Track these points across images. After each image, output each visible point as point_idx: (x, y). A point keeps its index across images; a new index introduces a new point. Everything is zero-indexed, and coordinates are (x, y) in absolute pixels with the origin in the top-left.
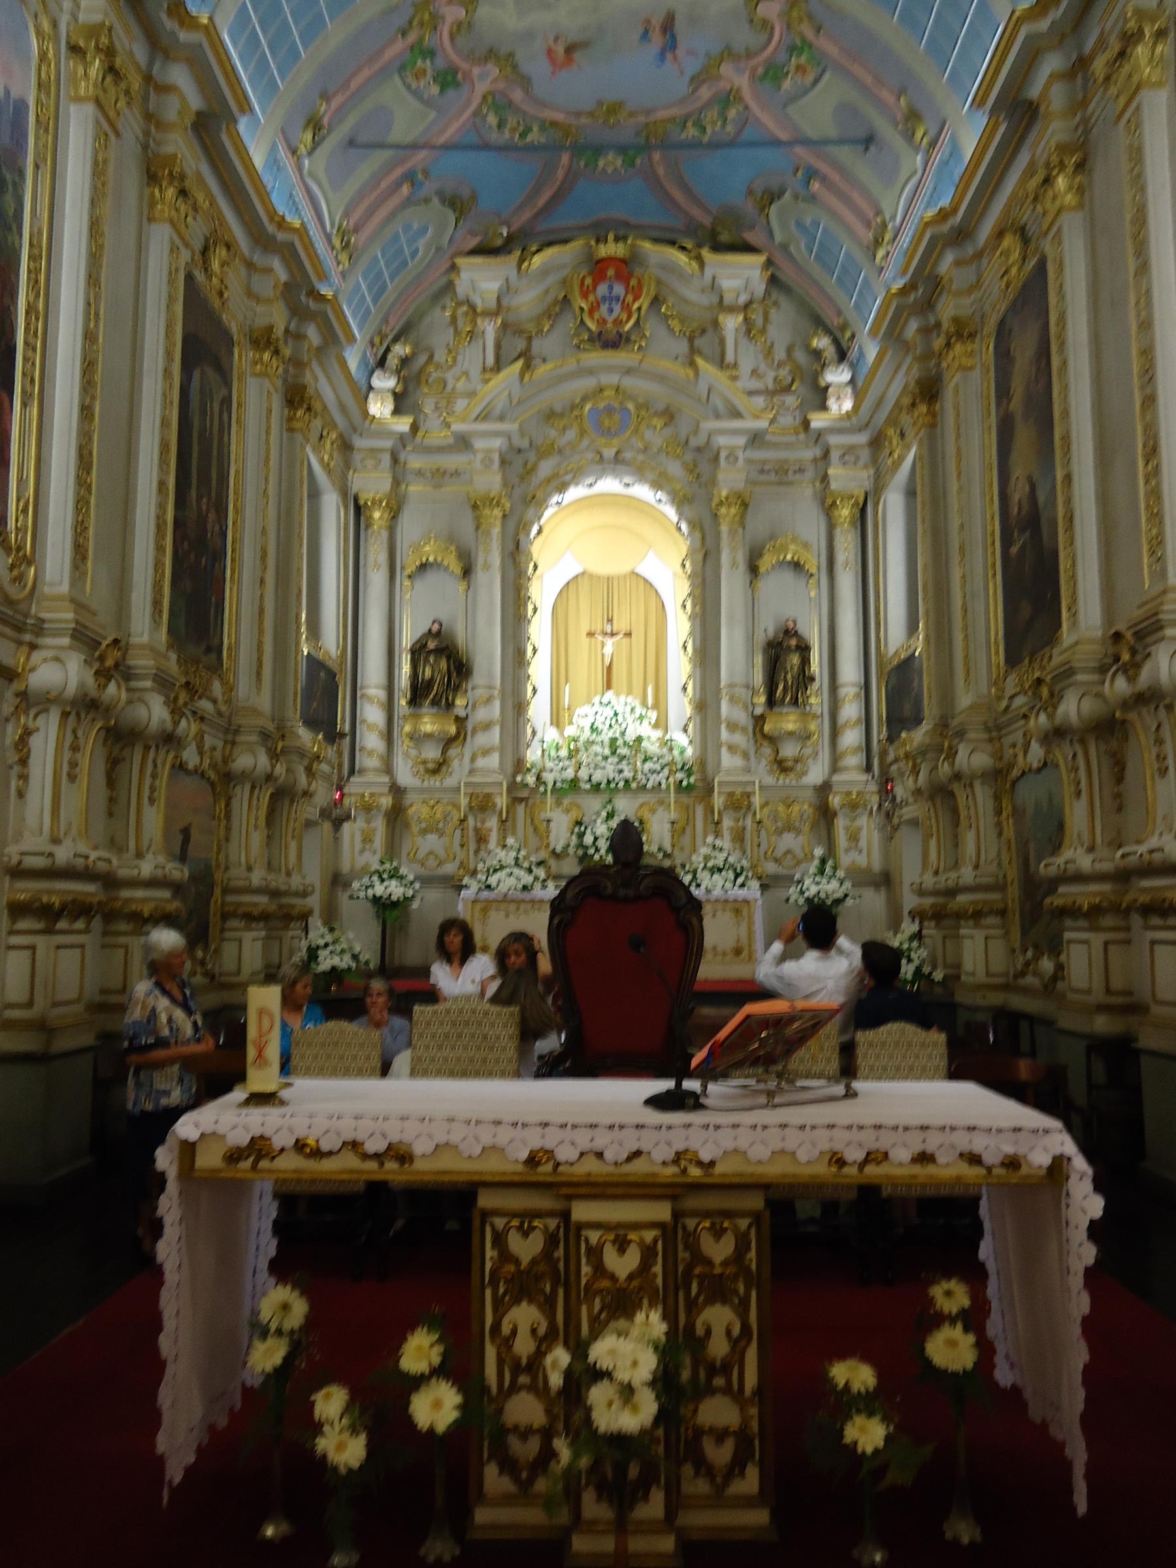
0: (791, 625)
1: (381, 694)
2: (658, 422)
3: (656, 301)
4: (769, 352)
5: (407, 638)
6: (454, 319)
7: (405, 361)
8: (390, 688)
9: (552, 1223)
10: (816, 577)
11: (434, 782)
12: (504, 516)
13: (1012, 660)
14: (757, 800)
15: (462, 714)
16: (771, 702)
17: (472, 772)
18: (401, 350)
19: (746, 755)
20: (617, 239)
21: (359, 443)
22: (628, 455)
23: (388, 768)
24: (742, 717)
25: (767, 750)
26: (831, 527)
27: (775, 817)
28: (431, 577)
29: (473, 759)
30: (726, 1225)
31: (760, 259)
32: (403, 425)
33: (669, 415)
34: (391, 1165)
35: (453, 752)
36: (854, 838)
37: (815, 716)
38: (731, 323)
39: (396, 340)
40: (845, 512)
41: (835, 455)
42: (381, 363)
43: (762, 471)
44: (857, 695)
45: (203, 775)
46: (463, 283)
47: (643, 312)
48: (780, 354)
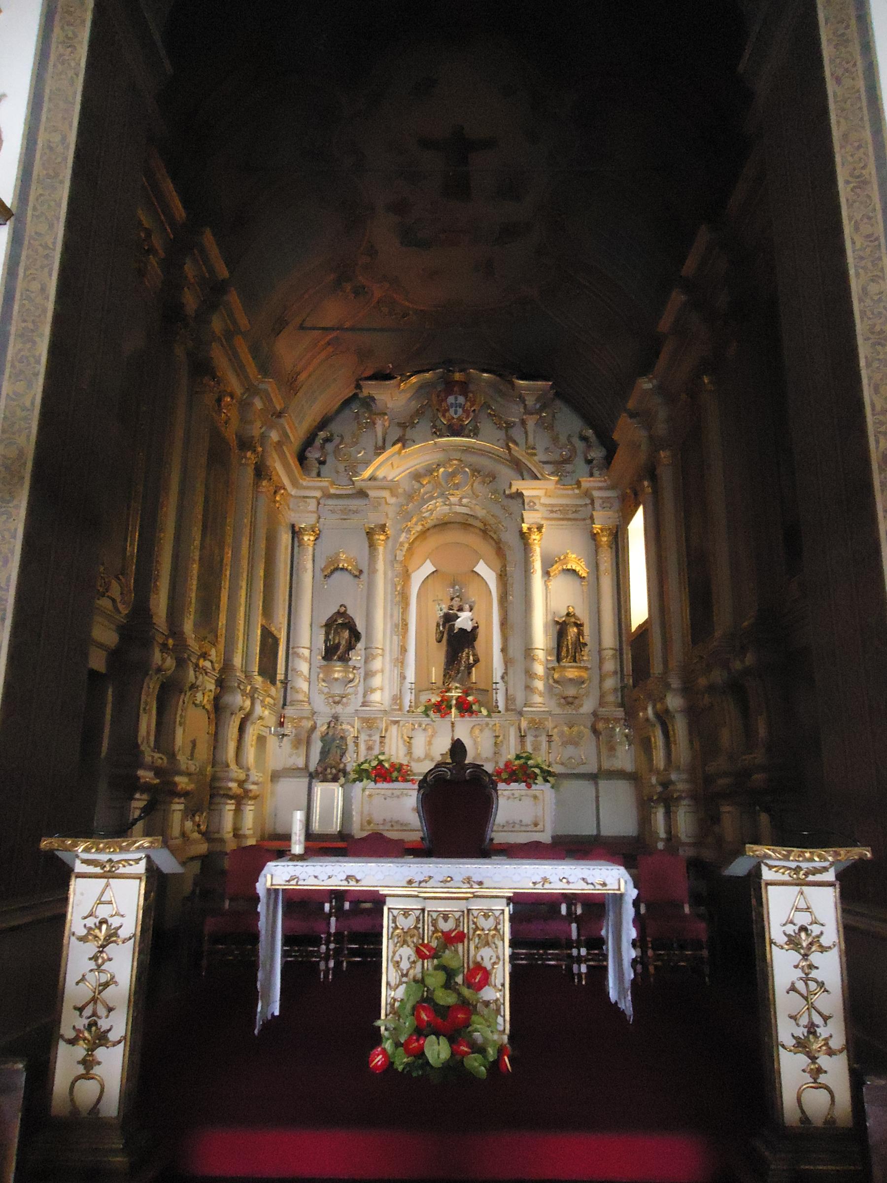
0: (571, 610)
2: (487, 479)
4: (555, 439)
9: (418, 912)
10: (587, 579)
11: (339, 709)
12: (388, 538)
13: (694, 642)
15: (358, 665)
16: (559, 660)
17: (364, 704)
20: (460, 371)
22: (465, 501)
26: (597, 547)
27: (562, 734)
29: (364, 697)
30: (490, 914)
34: (353, 883)
36: (612, 749)
37: (586, 668)
41: (597, 503)
43: (552, 512)
44: (614, 656)
45: (204, 707)
47: (477, 412)
48: (563, 439)
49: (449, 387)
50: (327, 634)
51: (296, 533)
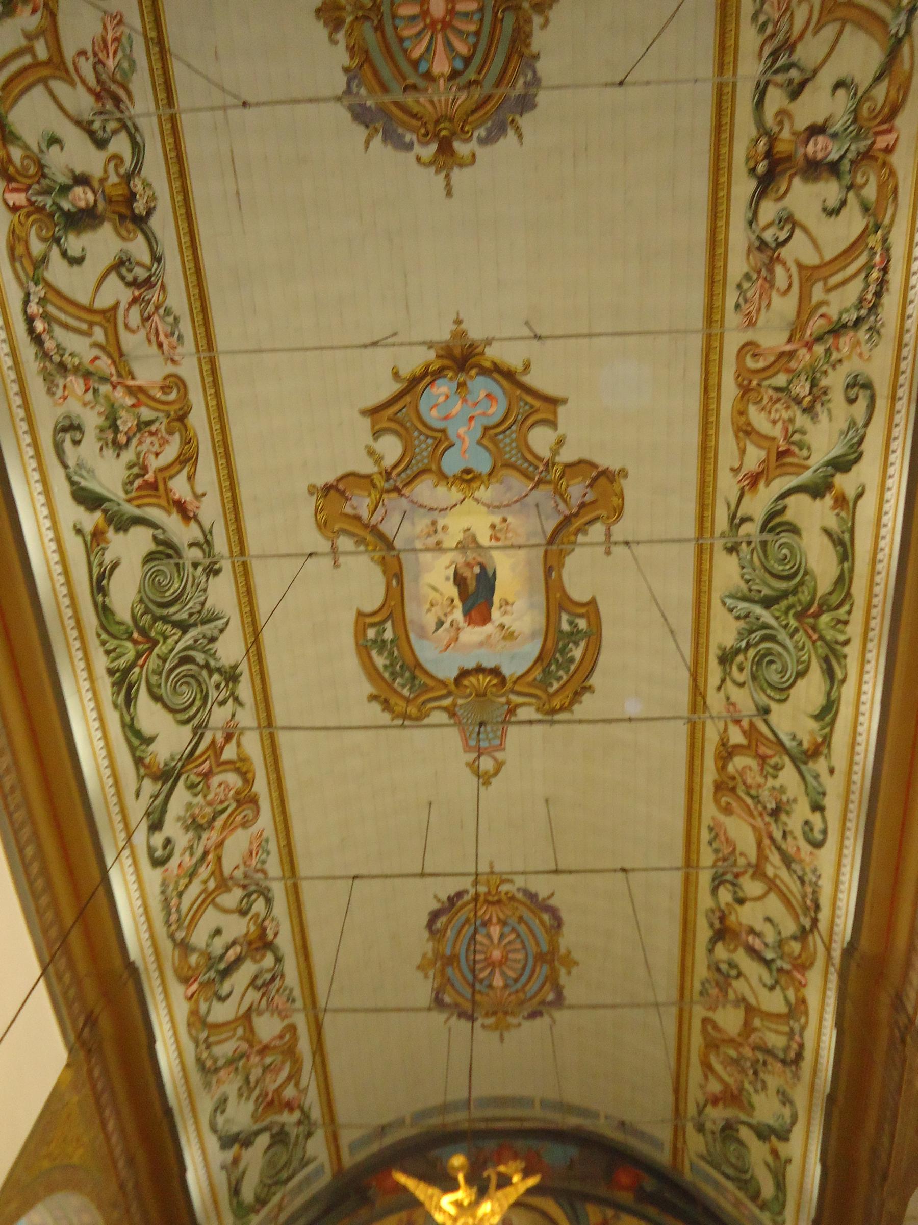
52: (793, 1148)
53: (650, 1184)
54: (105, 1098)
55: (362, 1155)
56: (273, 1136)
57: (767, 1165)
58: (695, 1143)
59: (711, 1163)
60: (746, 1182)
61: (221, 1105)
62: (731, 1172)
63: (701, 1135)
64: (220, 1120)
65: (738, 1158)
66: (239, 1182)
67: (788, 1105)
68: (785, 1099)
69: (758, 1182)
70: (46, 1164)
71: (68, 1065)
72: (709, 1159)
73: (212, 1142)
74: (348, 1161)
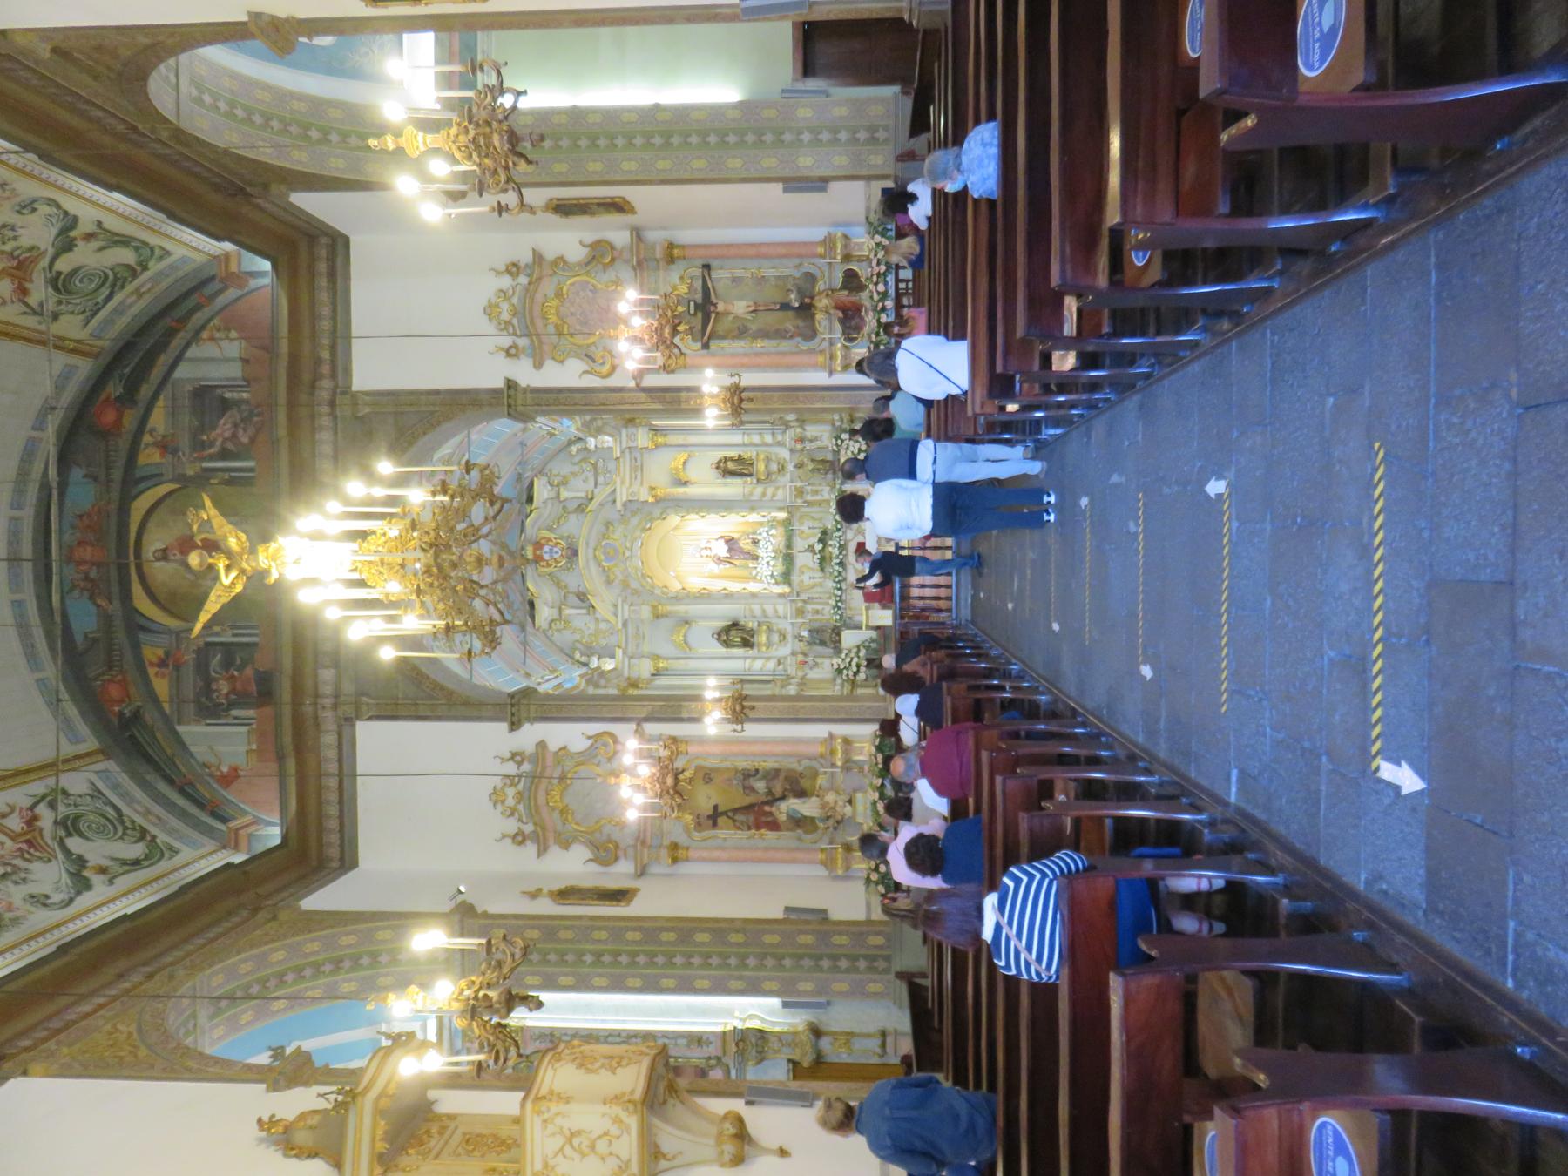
1: (748, 661)
3: (550, 529)
4: (574, 474)
5: (723, 651)
6: (558, 630)
7: (582, 655)
8: (745, 658)
11: (789, 637)
14: (799, 484)
16: (750, 475)
17: (786, 618)
18: (577, 656)
19: (777, 488)
21: (626, 674)
22: (628, 545)
23: (786, 658)
24: (759, 490)
25: (773, 477)
26: (666, 445)
28: (691, 640)
31: (536, 480)
32: (619, 653)
33: (608, 524)
35: (775, 628)
38: (564, 494)
39: (572, 658)
40: (660, 440)
41: (631, 444)
42: (586, 665)
46: (545, 626)
48: (576, 469)
49: (538, 559)
50: (734, 646)
51: (657, 673)
52: (87, 216)
53: (114, 389)
54: (56, 1024)
55: (83, 728)
56: (69, 835)
57: (101, 249)
58: (70, 326)
59: (93, 316)
60: (116, 279)
61: (41, 901)
62: (105, 292)
63: (61, 317)
64: (56, 898)
65: (91, 281)
66: (124, 863)
67: (35, 206)
68: (28, 207)
69: (119, 265)
70: (143, 1052)
71: (25, 1073)
72: (88, 314)
73: (85, 900)
74: (92, 744)
